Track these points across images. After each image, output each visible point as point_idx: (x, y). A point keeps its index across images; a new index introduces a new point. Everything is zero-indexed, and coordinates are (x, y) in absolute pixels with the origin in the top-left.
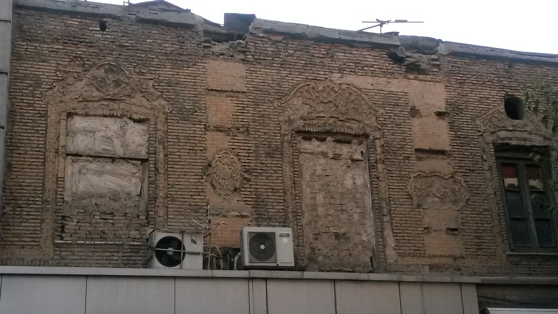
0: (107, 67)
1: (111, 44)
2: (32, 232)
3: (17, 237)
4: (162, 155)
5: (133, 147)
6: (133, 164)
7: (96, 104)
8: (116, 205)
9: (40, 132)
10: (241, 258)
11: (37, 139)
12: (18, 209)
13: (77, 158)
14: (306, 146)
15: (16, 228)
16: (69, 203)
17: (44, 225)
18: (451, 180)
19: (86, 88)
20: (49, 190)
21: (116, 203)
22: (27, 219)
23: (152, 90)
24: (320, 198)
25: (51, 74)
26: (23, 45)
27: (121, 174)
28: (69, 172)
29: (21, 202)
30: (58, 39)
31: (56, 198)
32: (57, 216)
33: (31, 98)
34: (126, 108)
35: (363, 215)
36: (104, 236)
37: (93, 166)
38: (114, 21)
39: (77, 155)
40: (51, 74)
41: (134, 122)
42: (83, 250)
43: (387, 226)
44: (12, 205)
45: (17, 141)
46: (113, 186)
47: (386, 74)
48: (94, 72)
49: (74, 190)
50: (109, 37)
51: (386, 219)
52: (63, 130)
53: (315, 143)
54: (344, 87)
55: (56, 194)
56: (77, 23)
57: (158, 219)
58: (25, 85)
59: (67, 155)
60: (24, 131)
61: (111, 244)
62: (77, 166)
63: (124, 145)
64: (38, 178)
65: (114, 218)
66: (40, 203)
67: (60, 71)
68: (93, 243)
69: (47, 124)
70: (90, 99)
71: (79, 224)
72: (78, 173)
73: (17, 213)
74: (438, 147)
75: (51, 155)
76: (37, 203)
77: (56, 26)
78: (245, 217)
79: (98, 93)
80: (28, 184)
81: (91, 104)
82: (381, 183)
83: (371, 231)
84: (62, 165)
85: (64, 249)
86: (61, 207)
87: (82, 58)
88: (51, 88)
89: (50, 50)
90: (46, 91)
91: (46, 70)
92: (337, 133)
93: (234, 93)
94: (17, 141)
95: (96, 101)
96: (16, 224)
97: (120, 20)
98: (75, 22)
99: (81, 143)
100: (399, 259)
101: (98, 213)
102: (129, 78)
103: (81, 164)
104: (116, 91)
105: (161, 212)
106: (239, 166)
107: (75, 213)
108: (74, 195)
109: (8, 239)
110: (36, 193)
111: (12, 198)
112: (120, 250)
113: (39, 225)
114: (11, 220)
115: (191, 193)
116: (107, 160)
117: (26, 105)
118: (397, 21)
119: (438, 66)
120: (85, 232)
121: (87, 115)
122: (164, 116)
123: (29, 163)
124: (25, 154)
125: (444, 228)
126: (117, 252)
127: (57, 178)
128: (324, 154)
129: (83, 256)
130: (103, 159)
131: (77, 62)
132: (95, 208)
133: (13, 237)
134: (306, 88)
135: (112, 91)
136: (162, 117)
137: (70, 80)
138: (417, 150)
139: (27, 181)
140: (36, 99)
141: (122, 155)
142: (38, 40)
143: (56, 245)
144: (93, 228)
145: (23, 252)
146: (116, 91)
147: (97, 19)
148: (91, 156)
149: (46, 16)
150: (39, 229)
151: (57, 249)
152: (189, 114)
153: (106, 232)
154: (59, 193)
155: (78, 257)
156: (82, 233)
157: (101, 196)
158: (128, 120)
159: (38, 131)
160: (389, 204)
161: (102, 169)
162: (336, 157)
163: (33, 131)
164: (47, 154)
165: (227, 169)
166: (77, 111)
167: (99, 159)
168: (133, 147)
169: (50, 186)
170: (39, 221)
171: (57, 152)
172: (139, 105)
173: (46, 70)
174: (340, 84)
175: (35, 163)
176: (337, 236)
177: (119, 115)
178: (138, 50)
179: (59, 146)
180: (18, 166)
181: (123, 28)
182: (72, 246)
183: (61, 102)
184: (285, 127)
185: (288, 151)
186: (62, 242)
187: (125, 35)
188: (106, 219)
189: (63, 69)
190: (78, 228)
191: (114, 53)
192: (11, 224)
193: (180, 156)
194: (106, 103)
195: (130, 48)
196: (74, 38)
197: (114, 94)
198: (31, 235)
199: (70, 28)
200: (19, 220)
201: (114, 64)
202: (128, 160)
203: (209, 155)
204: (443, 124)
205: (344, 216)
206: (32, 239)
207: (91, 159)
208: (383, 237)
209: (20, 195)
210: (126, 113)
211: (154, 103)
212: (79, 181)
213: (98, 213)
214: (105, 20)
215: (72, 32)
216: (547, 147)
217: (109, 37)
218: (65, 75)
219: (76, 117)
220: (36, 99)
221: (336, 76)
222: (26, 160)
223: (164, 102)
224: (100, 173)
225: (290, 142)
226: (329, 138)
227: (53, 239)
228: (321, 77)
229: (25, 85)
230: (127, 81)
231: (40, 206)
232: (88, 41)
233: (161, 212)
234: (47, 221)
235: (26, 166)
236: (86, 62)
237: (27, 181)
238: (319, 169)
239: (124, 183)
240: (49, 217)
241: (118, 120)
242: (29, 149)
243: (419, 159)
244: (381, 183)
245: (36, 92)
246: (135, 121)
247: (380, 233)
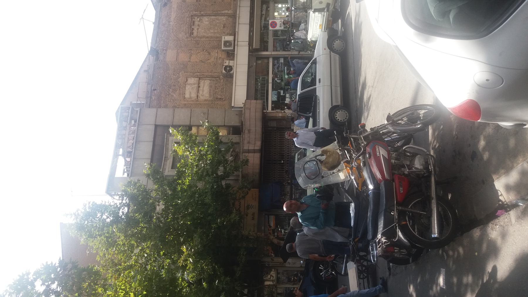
5: (195, 82)
10: (230, 50)
24: (212, 31)
35: (217, 19)
37: (201, 92)
43: (221, 12)
53: (194, 31)
63: (194, 84)
75: (198, 103)
83: (222, 17)
93: (178, 54)
98: (153, 98)
99: (194, 95)
128: (198, 29)
136: (186, 73)
157: (210, 90)
168: (195, 82)
169: (207, 103)
176: (224, 27)
185: (197, 39)
203: (198, 61)
205: (218, 24)
224: (203, 91)
238: (202, 31)
239: (206, 84)
247: (223, 15)
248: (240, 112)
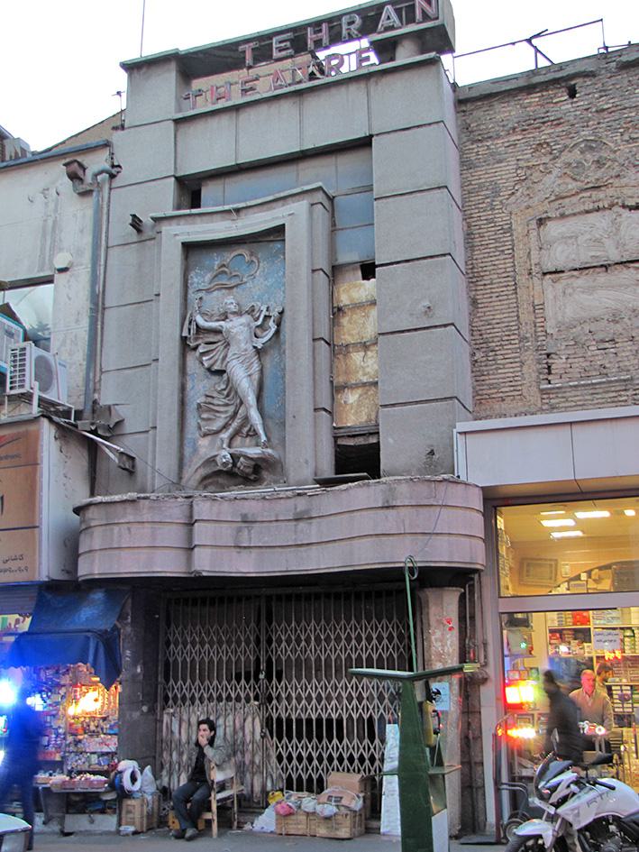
0: (583, 145)
1: (585, 112)
2: (512, 379)
3: (494, 388)
7: (574, 199)
8: (619, 327)
9: (506, 252)
11: (502, 262)
12: (491, 354)
13: (557, 275)
15: (491, 377)
16: (555, 337)
17: (525, 369)
19: (560, 182)
20: (526, 323)
21: (618, 325)
22: (503, 364)
25: (511, 175)
26: (473, 149)
27: (620, 286)
28: (550, 296)
29: (494, 344)
30: (514, 129)
31: (535, 332)
32: (541, 355)
33: (490, 212)
34: (615, 194)
36: (605, 371)
37: (582, 281)
38: (586, 79)
39: (556, 272)
40: (511, 175)
41: (630, 210)
42: (579, 393)
44: (484, 350)
45: (480, 269)
46: (612, 304)
48: (566, 157)
49: (560, 318)
50: (582, 103)
52: (534, 244)
55: (535, 326)
56: (537, 99)
58: (480, 197)
59: (545, 274)
60: (486, 255)
61: (616, 381)
62: (559, 286)
64: (510, 310)
65: (617, 345)
66: (517, 341)
67: (522, 168)
68: (589, 382)
69: (513, 240)
70: (565, 194)
71: (570, 361)
72: (562, 295)
73: (490, 359)
76: (513, 342)
77: (510, 111)
79: (574, 184)
80: (498, 321)
81: (567, 200)
84: (538, 288)
85: (554, 396)
86: (544, 343)
87: (548, 144)
88: (513, 193)
89: (506, 144)
90: (508, 199)
91: (504, 173)
94: (480, 269)
95: (573, 195)
96: (491, 372)
97: (594, 76)
98: (535, 98)
99: (560, 256)
101: (594, 343)
102: (615, 152)
103: (564, 282)
104: (599, 174)
107: (563, 347)
108: (559, 325)
109: (484, 392)
110: (510, 330)
111: (482, 341)
112: (629, 386)
113: (519, 369)
114: (485, 368)
116: (598, 270)
117: (485, 222)
120: (578, 370)
121: (563, 216)
123: (497, 294)
124: (492, 284)
126: (625, 390)
129: (580, 400)
130: (592, 270)
131: (543, 151)
132: (590, 336)
133: (490, 389)
135: (593, 176)
139: (498, 316)
140: (497, 211)
141: (618, 259)
142: (490, 137)
143: (542, 391)
144: (588, 364)
145: (503, 405)
146: (599, 174)
147: (563, 84)
148: (576, 270)
149: (495, 103)
150: (519, 374)
151: (545, 396)
153: (607, 366)
154: (538, 325)
156: (575, 372)
158: (621, 210)
159: (503, 251)
161: (595, 284)
163: (498, 253)
166: (549, 215)
167: (587, 271)
169: (526, 317)
170: (518, 364)
171: (530, 274)
173: (504, 173)
175: (504, 293)
177: (606, 206)
178: (625, 108)
179: (531, 265)
180: (484, 300)
181: (600, 85)
182: (563, 390)
183: (528, 207)
186: (550, 386)
187: (603, 94)
188: (605, 349)
189: (525, 165)
190: (569, 366)
191: (591, 123)
192: (485, 373)
194: (588, 194)
195: (613, 109)
196: (535, 120)
197: (598, 180)
198: (511, 384)
199: (528, 109)
200: (494, 367)
201: (592, 138)
202: (628, 264)
206: (512, 388)
207: (575, 273)
209: (491, 335)
210: (616, 201)
212: (564, 305)
213: (594, 343)
214: (573, 83)
215: (531, 113)
217: (582, 103)
218: (529, 172)
219: (549, 223)
220: (497, 211)
222: (493, 290)
224: (590, 290)
227: (539, 383)
229: (480, 197)
230: (612, 156)
231: (517, 346)
232: (552, 118)
234: (528, 362)
235: (494, 299)
236: (554, 147)
237: (498, 316)
240: (530, 357)
241: (607, 212)
242: (496, 276)
245: (494, 203)
248: (438, 466)
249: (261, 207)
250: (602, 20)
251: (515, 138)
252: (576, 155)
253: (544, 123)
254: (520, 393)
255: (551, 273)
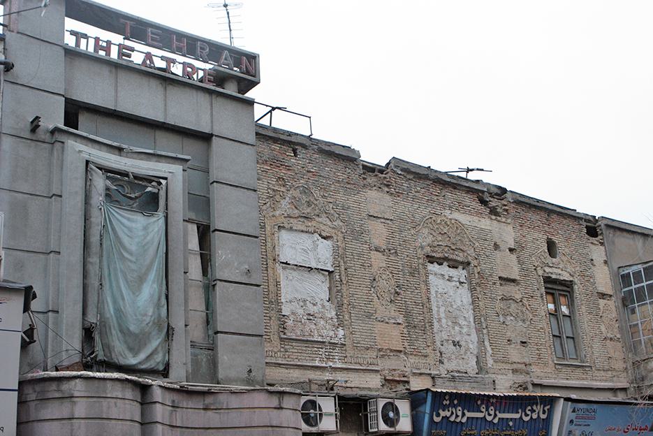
4: (343, 268)
6: (323, 274)
14: (434, 268)
18: (521, 304)
23: (332, 212)
30: (266, 161)
37: (295, 274)
39: (286, 263)
42: (299, 345)
43: (486, 337)
47: (479, 214)
51: (485, 331)
54: (453, 221)
57: (345, 323)
74: (512, 277)
75: (270, 262)
78: (399, 324)
82: (480, 303)
89: (262, 169)
92: (451, 260)
98: (276, 147)
100: (495, 364)
102: (316, 200)
105: (347, 317)
106: (393, 282)
115: (365, 302)
118: (478, 169)
119: (507, 210)
121: (291, 229)
122: (342, 235)
125: (519, 342)
127: (277, 282)
134: (430, 220)
137: (277, 198)
138: (500, 278)
143: (281, 339)
146: (309, 210)
151: (282, 343)
152: (358, 234)
155: (296, 351)
160: (485, 320)
162: (450, 279)
164: (268, 261)
165: (385, 284)
172: (324, 223)
174: (451, 219)
184: (419, 251)
193: (355, 269)
203: (374, 269)
204: (513, 257)
207: (295, 267)
208: (484, 346)
211: (334, 223)
216: (571, 281)
221: (447, 212)
223: (341, 224)
225: (423, 265)
226: (445, 264)
228: (438, 212)
230: (315, 202)
232: (286, 164)
233: (347, 317)
243: (501, 285)
244: (480, 303)
246: (324, 238)
247: (481, 342)
249: (147, 156)
250: (310, 117)
251: (267, 167)
252: (296, 193)
253: (281, 165)
254: (268, 337)
255: (283, 263)
